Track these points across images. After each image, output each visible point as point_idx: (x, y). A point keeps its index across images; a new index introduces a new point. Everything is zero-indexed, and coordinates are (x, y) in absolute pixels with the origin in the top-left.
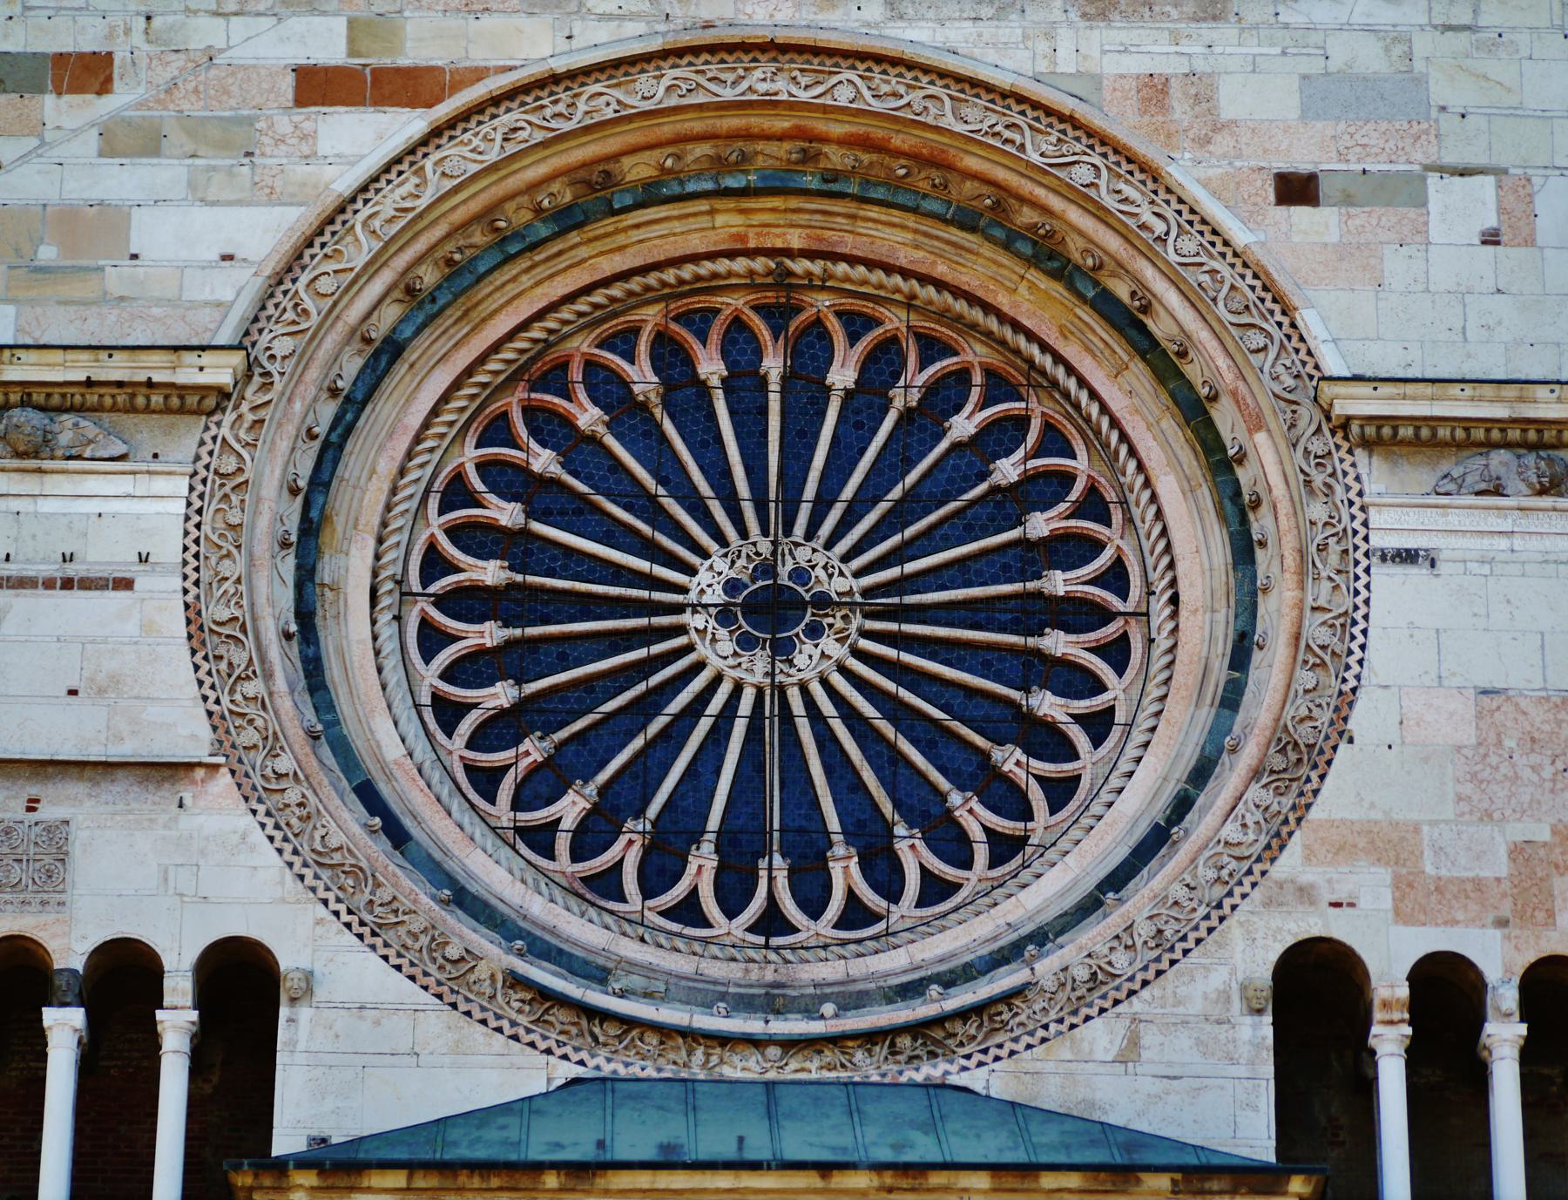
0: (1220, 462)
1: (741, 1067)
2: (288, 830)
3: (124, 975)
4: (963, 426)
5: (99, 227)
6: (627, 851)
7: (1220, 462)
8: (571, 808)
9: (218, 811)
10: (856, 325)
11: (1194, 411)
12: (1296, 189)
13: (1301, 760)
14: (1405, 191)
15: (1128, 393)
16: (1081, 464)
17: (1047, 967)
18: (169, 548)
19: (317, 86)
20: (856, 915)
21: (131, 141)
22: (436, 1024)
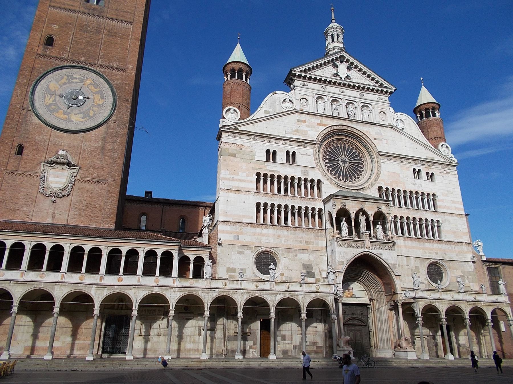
0: (371, 156)
1: (349, 190)
2: (321, 172)
3: (312, 181)
4: (354, 151)
5: (306, 132)
6: (337, 176)
7: (371, 156)
8: (333, 173)
9: (317, 171)
10: (347, 144)
11: (369, 152)
12: (375, 139)
13: (378, 175)
14: (381, 140)
15: (364, 150)
16: (361, 154)
17: (365, 186)
18: (313, 153)
19: (318, 124)
20: (350, 181)
21: (308, 126)
22: (331, 186)
